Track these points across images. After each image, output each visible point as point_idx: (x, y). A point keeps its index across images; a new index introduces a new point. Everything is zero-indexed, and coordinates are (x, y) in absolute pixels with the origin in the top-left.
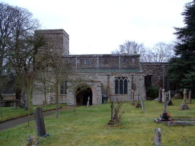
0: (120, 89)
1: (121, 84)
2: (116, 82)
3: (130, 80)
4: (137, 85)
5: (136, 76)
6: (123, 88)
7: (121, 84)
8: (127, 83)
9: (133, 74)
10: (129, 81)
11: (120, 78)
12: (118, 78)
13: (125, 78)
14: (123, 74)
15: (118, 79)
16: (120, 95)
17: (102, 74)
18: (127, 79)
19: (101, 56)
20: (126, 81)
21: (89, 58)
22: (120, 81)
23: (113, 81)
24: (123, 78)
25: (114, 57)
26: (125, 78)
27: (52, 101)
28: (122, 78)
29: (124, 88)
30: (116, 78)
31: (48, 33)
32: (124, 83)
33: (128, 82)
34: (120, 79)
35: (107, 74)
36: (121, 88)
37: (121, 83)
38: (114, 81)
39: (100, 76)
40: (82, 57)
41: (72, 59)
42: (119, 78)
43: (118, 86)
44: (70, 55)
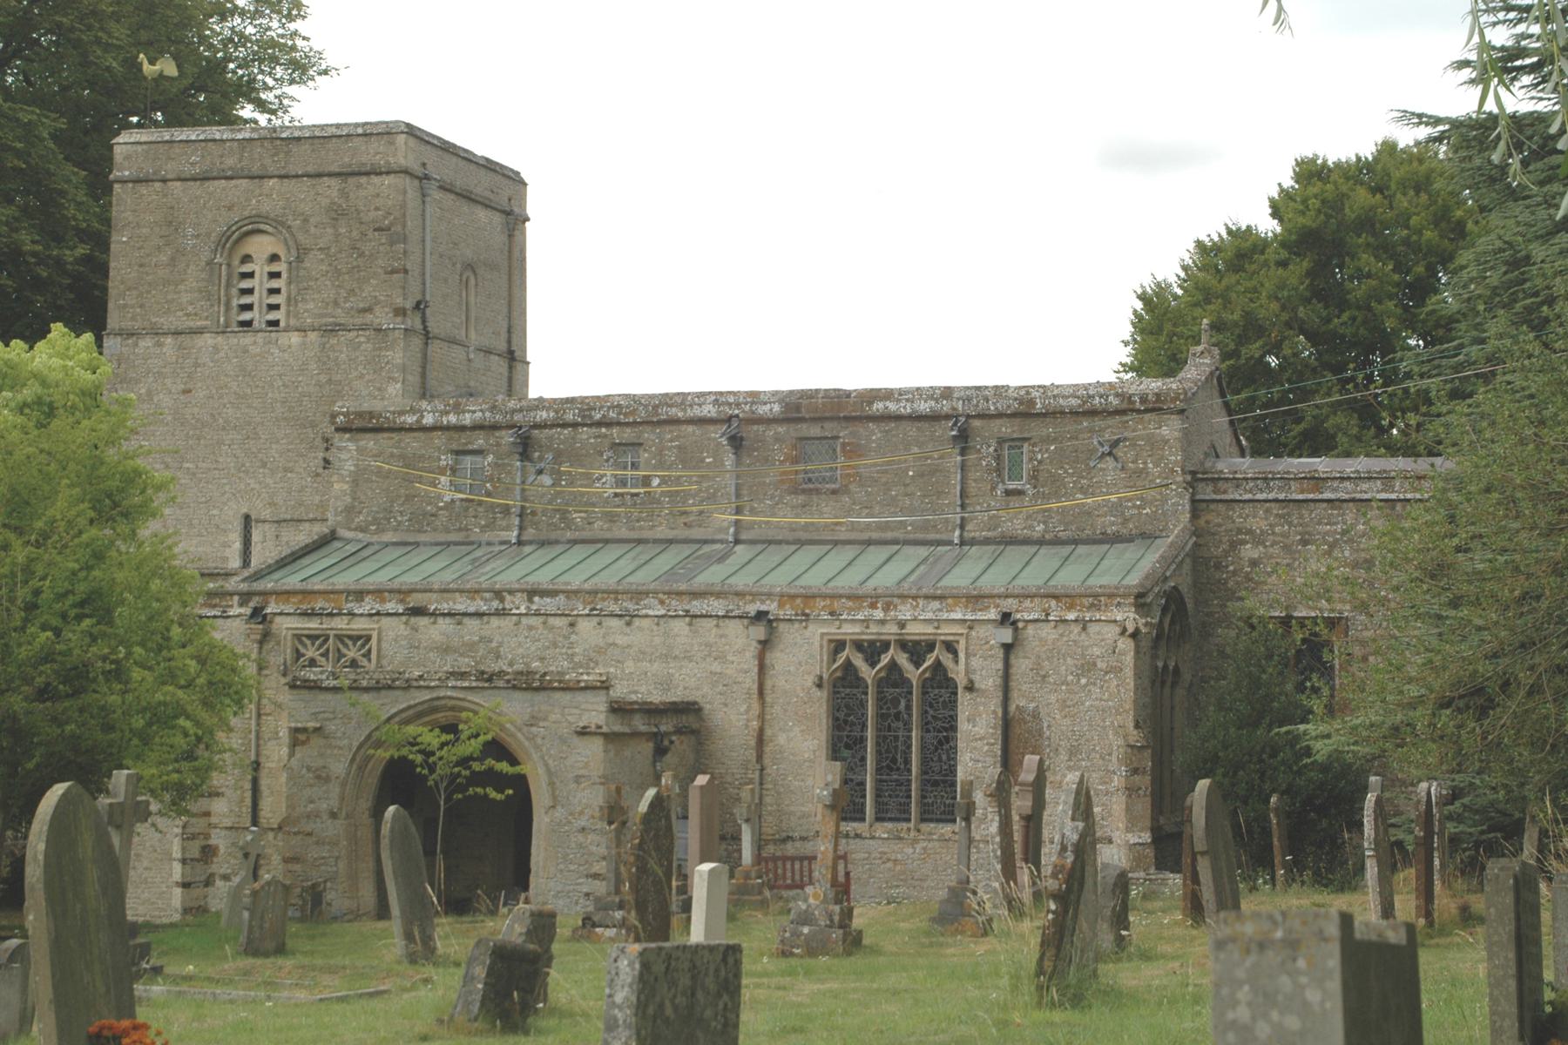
0: (879, 770)
1: (891, 717)
2: (843, 686)
3: (988, 680)
4: (1056, 725)
5: (1048, 632)
6: (907, 761)
7: (891, 717)
8: (952, 704)
9: (1009, 604)
10: (970, 688)
11: (886, 646)
12: (858, 646)
13: (931, 646)
14: (905, 612)
15: (859, 661)
16: (882, 830)
17: (697, 606)
18: (947, 660)
19: (763, 410)
20: (939, 679)
21: (648, 435)
22: (880, 683)
23: (810, 680)
24: (917, 650)
25: (898, 418)
26: (931, 646)
27: (208, 883)
28: (903, 645)
29: (924, 761)
30: (839, 646)
31: (255, 170)
32: (880, 699)
33: (963, 699)
34: (885, 660)
35: (752, 609)
36: (891, 761)
37: (896, 702)
38: (819, 686)
39: (680, 626)
40: (575, 425)
41: (480, 442)
42: (872, 650)
43: (863, 740)
44: (541, 403)
